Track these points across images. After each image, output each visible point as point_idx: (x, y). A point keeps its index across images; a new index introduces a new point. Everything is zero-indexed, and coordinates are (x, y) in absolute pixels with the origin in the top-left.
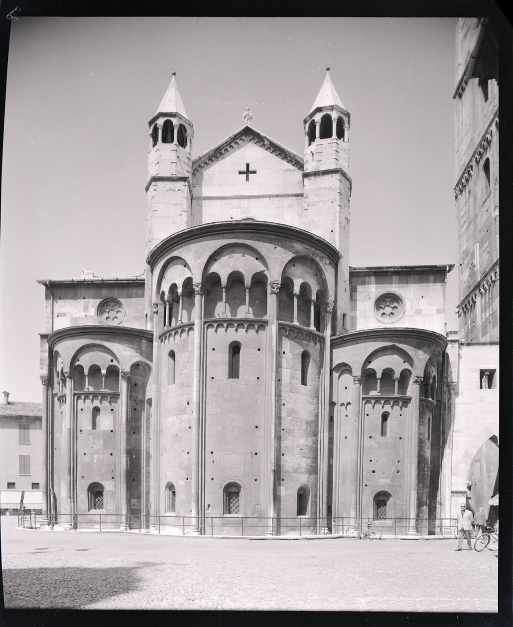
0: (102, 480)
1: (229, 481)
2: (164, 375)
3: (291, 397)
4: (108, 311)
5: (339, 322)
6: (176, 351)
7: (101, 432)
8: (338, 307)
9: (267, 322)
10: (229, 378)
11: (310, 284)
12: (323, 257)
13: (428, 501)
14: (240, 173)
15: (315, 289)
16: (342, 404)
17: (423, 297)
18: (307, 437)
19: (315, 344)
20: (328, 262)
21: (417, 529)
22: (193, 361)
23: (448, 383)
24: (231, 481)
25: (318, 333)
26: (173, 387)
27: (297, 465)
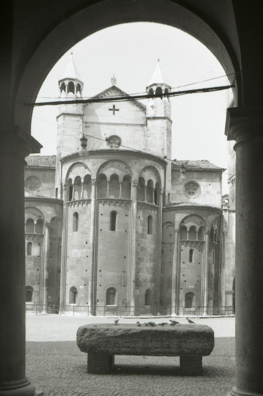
0: (33, 284)
1: (113, 287)
2: (70, 225)
3: (143, 241)
4: (30, 183)
5: (167, 198)
6: (79, 213)
7: (33, 257)
8: (166, 190)
9: (131, 201)
10: (110, 230)
11: (152, 180)
12: (159, 166)
13: (213, 297)
14: (110, 110)
15: (155, 181)
16: (168, 244)
17: (210, 185)
18: (150, 262)
19: (155, 211)
20: (161, 168)
21: (207, 313)
22: (90, 220)
23: (223, 232)
24: (111, 287)
25: (156, 206)
26: (76, 234)
27: (145, 278)
